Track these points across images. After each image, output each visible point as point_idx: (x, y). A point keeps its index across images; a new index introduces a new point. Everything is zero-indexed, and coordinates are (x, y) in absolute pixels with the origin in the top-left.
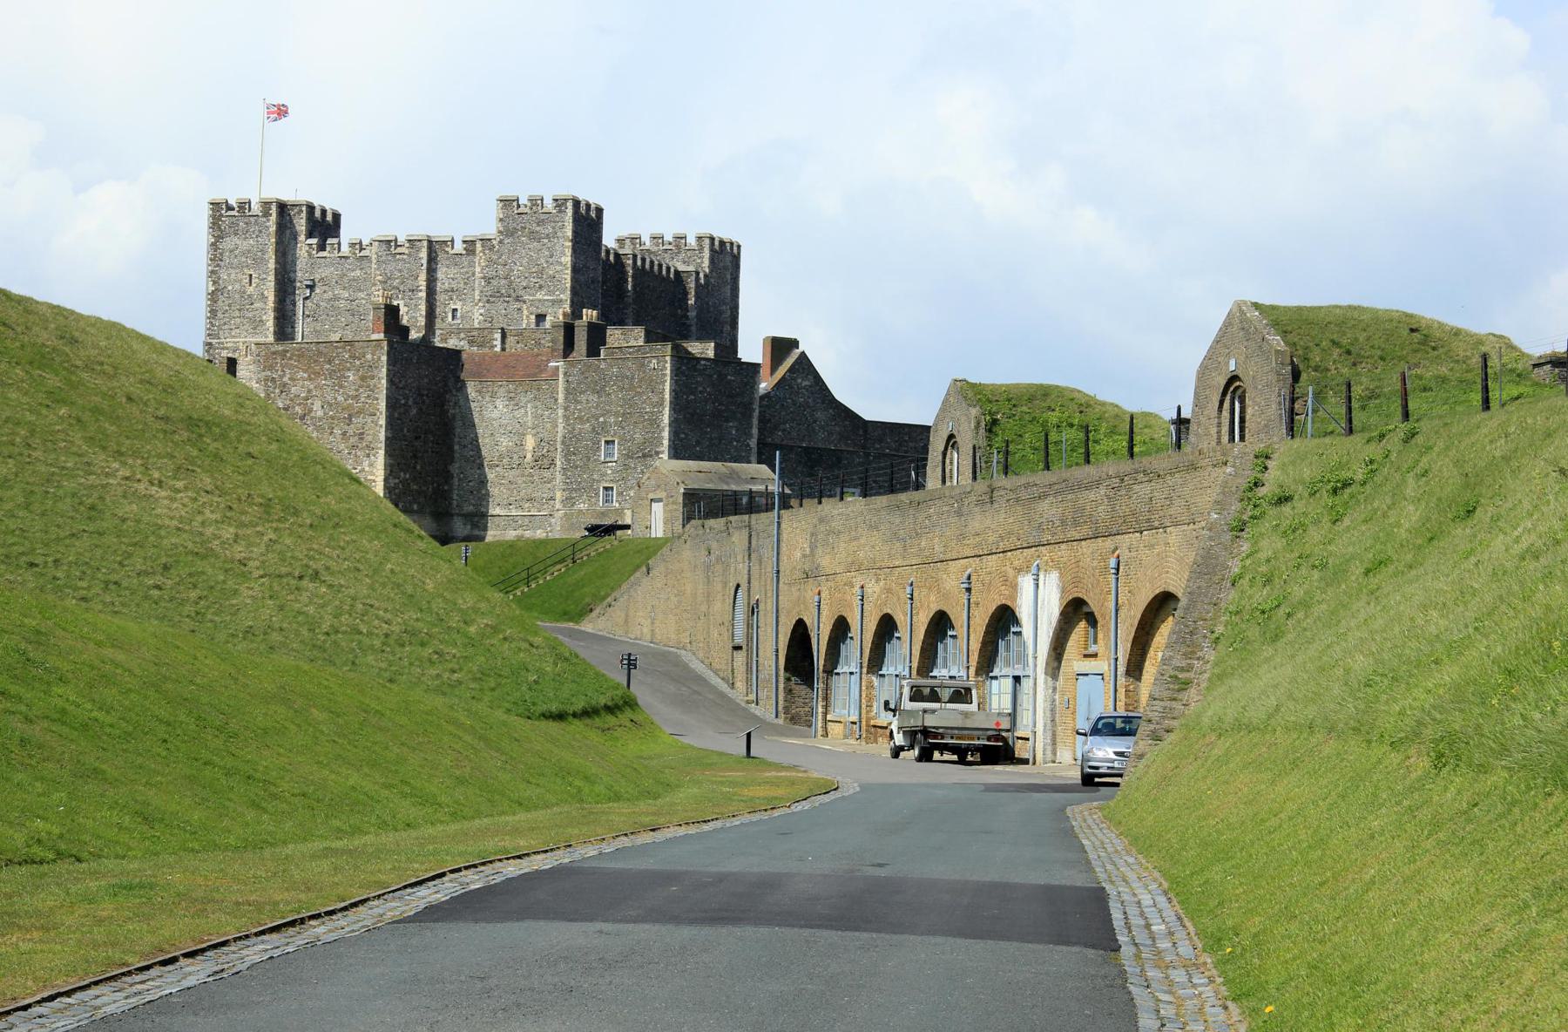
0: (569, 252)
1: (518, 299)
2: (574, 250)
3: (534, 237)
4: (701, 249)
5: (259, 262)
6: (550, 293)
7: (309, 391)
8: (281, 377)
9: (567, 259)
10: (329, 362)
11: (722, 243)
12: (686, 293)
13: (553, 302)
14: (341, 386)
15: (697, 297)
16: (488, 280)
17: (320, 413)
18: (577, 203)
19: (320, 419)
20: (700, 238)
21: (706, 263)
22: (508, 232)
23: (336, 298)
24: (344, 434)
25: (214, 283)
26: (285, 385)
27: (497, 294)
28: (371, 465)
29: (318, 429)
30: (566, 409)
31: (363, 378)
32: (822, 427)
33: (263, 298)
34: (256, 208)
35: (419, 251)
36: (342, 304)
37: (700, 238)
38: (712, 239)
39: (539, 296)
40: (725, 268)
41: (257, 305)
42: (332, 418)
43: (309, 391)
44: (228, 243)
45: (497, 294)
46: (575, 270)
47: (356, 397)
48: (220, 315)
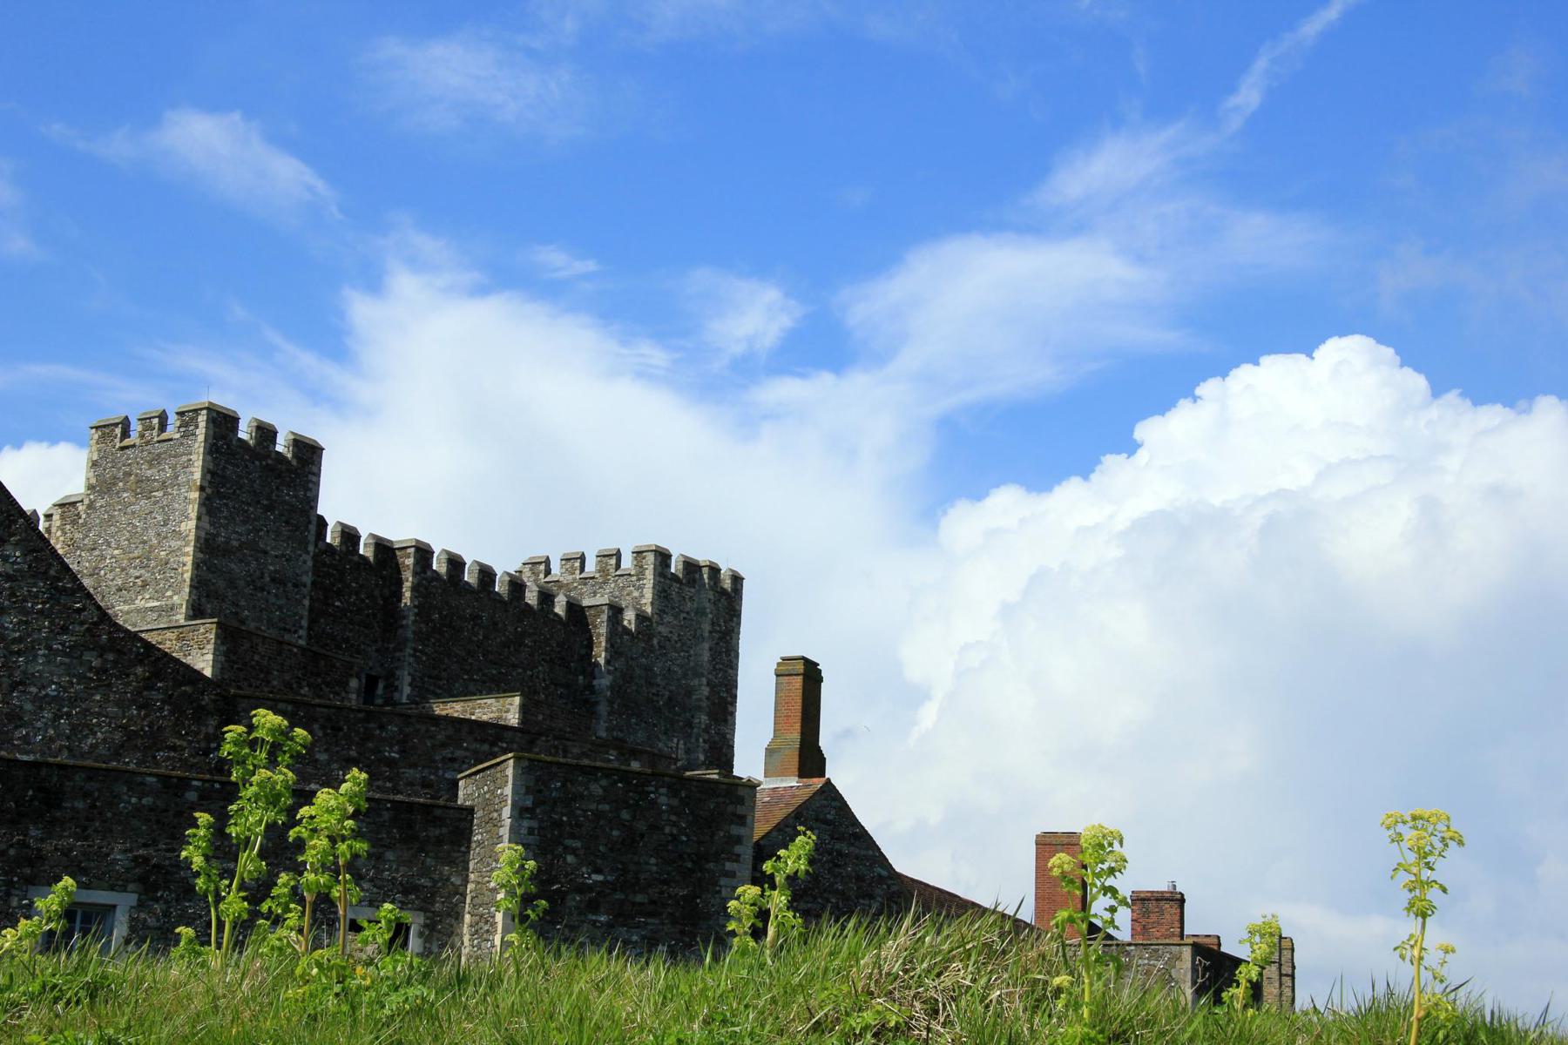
0: (193, 511)
2: (209, 506)
3: (143, 488)
4: (640, 574)
6: (160, 594)
9: (189, 526)
11: (691, 566)
12: (590, 645)
15: (614, 650)
18: (223, 422)
20: (639, 554)
21: (648, 595)
32: (41, 702)
37: (639, 554)
38: (663, 557)
40: (701, 612)
46: (207, 546)
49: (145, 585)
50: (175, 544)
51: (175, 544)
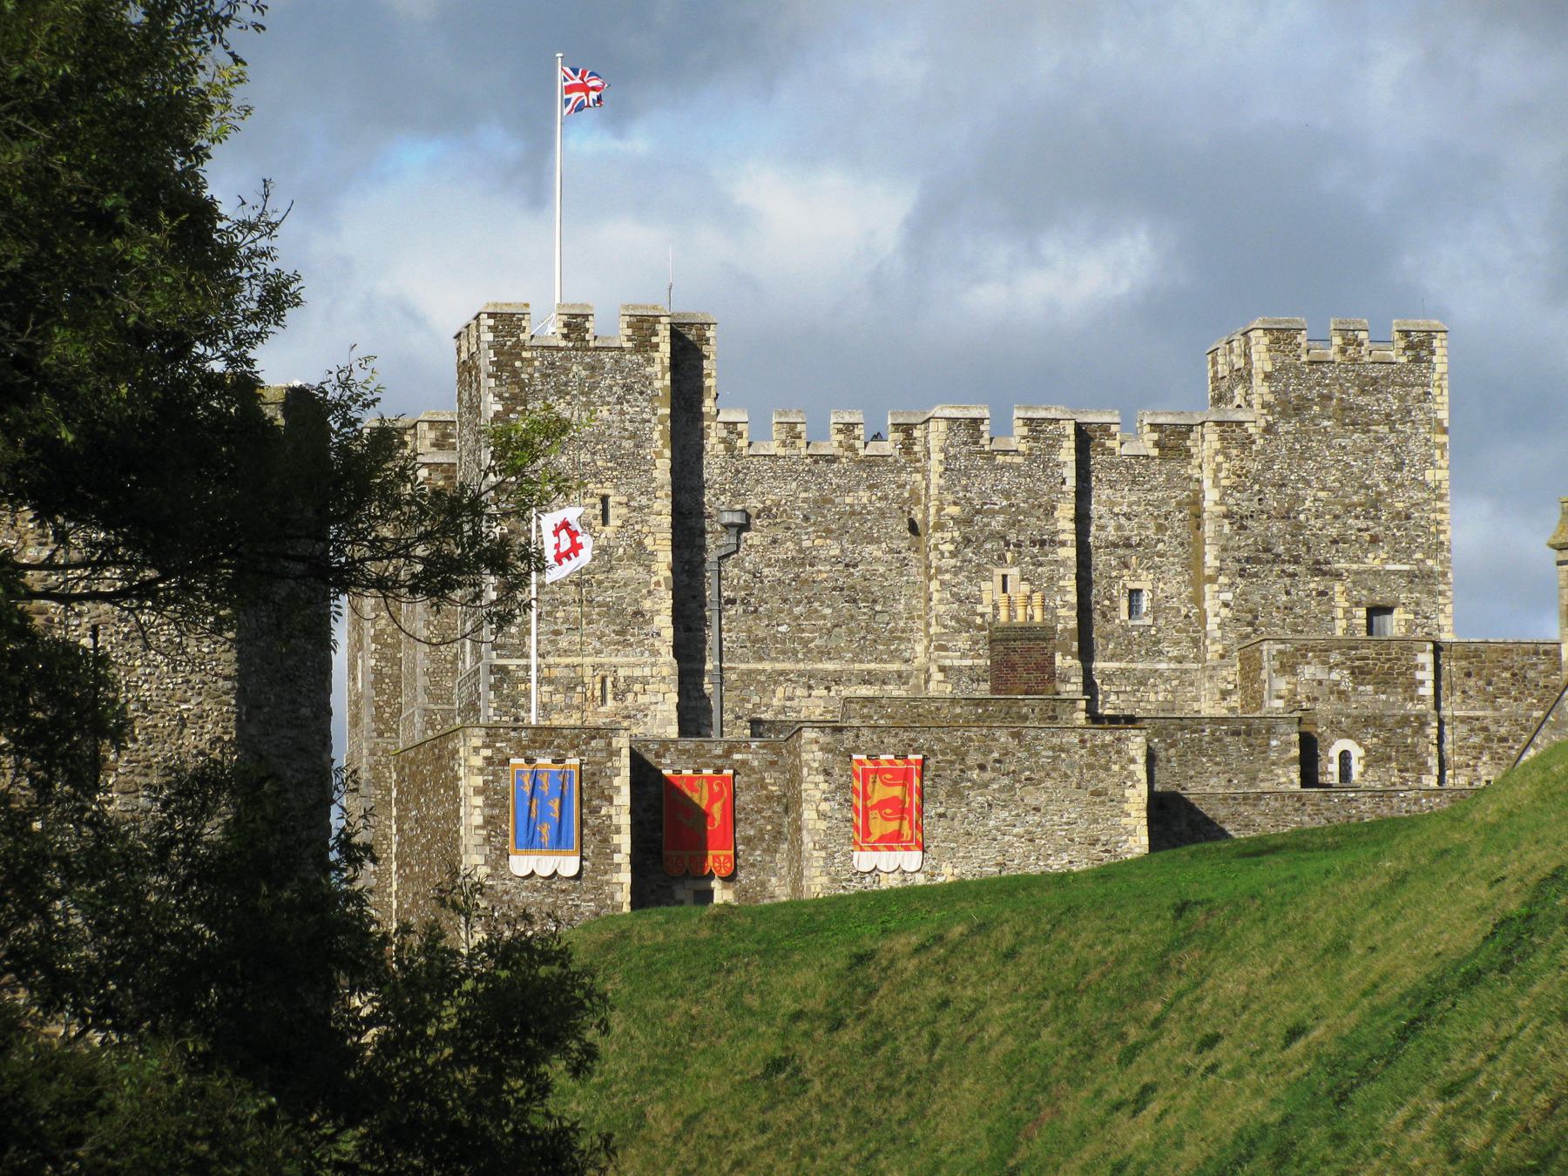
1: (1318, 569)
5: (630, 463)
13: (1411, 577)
16: (1240, 522)
22: (1289, 407)
23: (806, 559)
27: (1264, 554)
33: (641, 554)
34: (610, 328)
35: (1055, 444)
36: (823, 571)
39: (1373, 561)
45: (1264, 554)
49: (1374, 540)
50: (1419, 496)
51: (1419, 496)
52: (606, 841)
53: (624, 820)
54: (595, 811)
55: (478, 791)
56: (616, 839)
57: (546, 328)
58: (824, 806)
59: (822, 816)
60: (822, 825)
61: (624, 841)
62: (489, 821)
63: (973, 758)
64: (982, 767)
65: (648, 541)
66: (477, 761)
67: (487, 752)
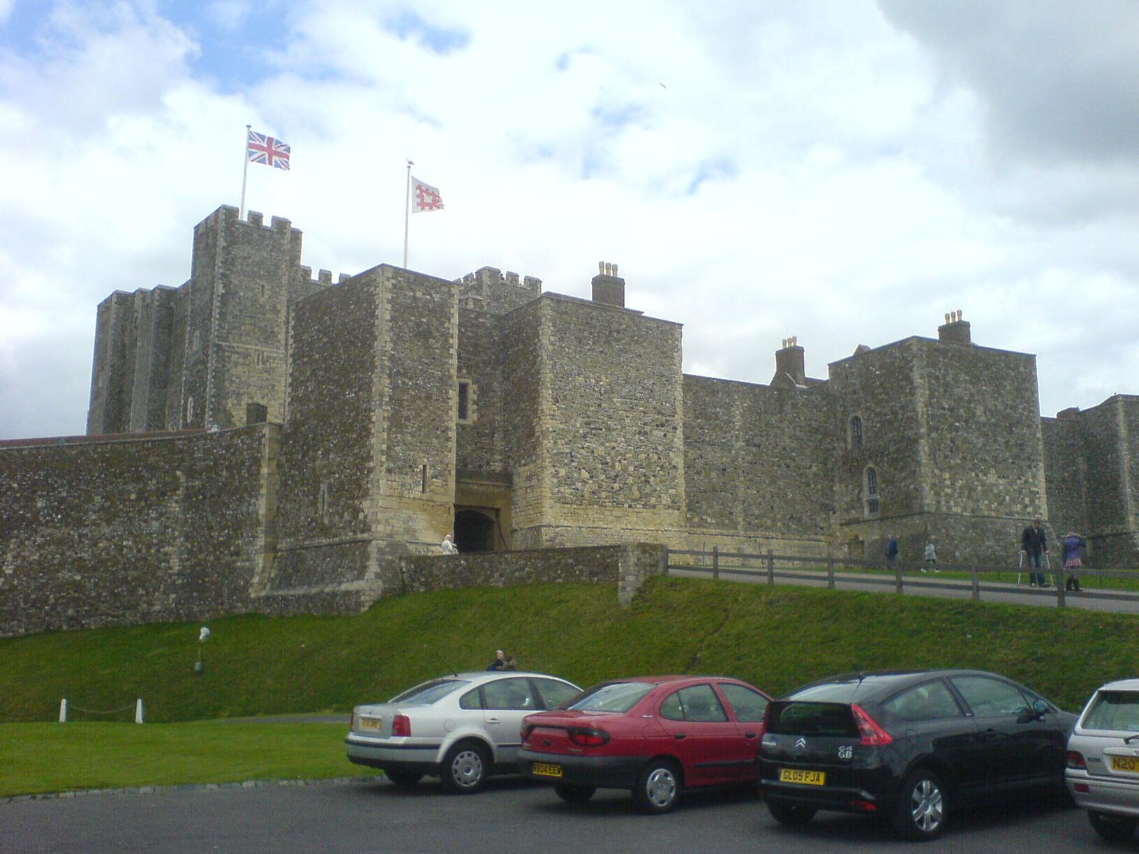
7: (972, 395)
8: (944, 376)
10: (987, 369)
14: (1000, 395)
17: (983, 419)
19: (984, 425)
24: (1007, 443)
25: (225, 286)
26: (947, 385)
28: (1034, 477)
29: (985, 435)
30: (1131, 443)
31: (1018, 390)
33: (275, 311)
41: (268, 316)
42: (995, 425)
43: (972, 395)
44: (241, 251)
47: (1014, 408)
48: (229, 318)
52: (446, 341)
53: (456, 331)
54: (442, 324)
55: (389, 302)
56: (451, 341)
57: (244, 217)
58: (552, 338)
59: (552, 344)
60: (551, 348)
61: (454, 341)
62: (393, 319)
63: (615, 326)
64: (618, 332)
65: (278, 306)
66: (389, 285)
67: (394, 281)
